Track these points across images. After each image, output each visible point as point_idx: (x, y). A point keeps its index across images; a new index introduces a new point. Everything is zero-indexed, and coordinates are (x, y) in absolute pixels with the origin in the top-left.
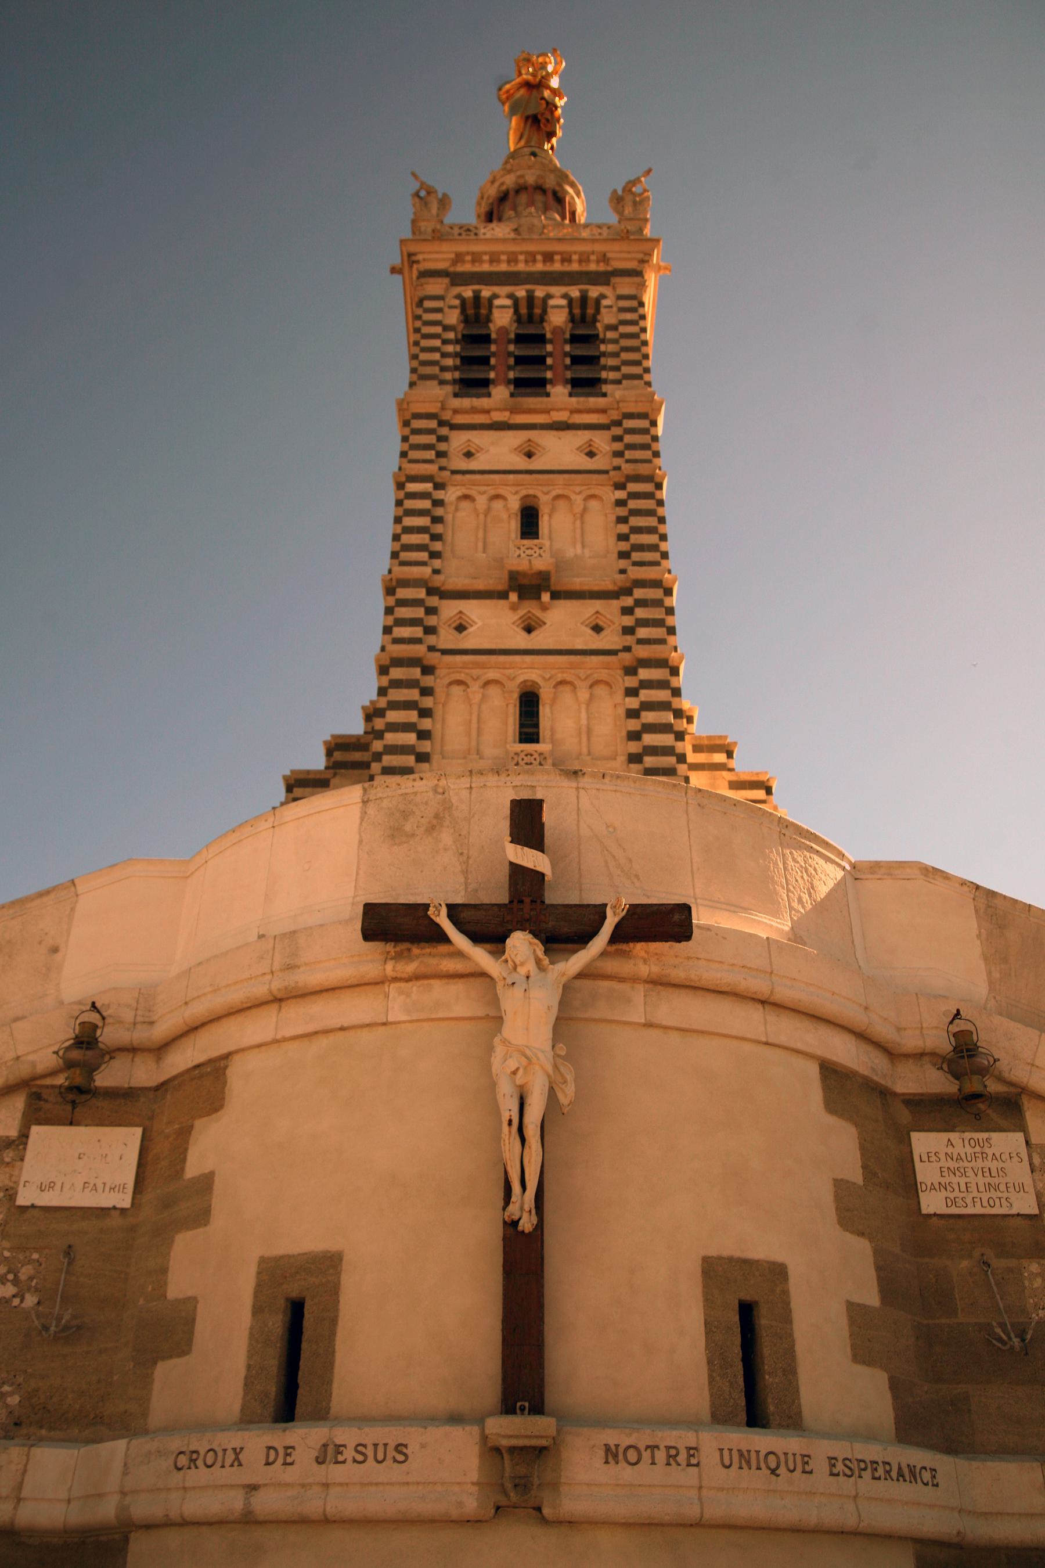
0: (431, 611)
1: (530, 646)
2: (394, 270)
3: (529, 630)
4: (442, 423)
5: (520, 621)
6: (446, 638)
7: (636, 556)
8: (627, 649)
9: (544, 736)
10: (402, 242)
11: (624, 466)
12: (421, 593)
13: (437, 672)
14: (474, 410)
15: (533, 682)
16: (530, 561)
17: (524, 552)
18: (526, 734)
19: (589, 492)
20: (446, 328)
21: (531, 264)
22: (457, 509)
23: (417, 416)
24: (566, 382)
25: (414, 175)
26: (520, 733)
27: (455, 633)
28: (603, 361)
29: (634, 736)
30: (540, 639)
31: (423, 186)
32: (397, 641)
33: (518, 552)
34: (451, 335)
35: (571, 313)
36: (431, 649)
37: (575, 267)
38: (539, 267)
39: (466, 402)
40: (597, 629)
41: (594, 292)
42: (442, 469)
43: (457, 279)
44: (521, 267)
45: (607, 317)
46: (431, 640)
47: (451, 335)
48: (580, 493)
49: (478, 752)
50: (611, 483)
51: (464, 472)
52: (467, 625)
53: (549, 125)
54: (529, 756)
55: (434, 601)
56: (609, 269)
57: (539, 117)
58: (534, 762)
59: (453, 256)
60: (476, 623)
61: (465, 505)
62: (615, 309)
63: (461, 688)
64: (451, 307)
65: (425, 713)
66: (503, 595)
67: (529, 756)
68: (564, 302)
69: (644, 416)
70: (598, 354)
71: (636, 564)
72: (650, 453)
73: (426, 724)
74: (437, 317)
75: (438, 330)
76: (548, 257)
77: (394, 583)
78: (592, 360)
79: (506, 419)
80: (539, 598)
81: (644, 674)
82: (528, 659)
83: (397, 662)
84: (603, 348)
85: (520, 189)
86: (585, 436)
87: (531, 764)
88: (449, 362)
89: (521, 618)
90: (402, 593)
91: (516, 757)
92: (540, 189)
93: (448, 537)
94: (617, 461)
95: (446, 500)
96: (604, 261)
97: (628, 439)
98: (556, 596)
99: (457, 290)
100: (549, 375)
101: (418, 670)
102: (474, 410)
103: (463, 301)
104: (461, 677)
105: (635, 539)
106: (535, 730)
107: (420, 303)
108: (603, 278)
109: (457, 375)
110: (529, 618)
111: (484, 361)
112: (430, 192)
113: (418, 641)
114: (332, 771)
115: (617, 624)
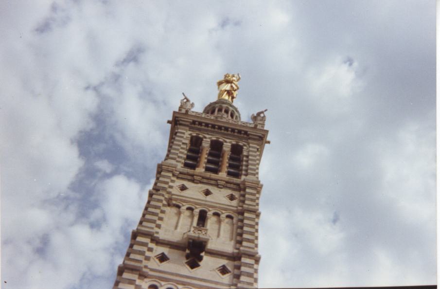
0: (150, 250)
2: (169, 122)
10: (174, 112)
14: (188, 174)
20: (183, 143)
25: (183, 94)
28: (241, 168)
31: (186, 98)
36: (146, 267)
43: (191, 129)
47: (184, 146)
55: (151, 245)
59: (191, 121)
69: (255, 188)
78: (238, 167)
90: (139, 239)
99: (190, 132)
103: (192, 137)
107: (176, 133)
112: (188, 101)
115: (232, 272)
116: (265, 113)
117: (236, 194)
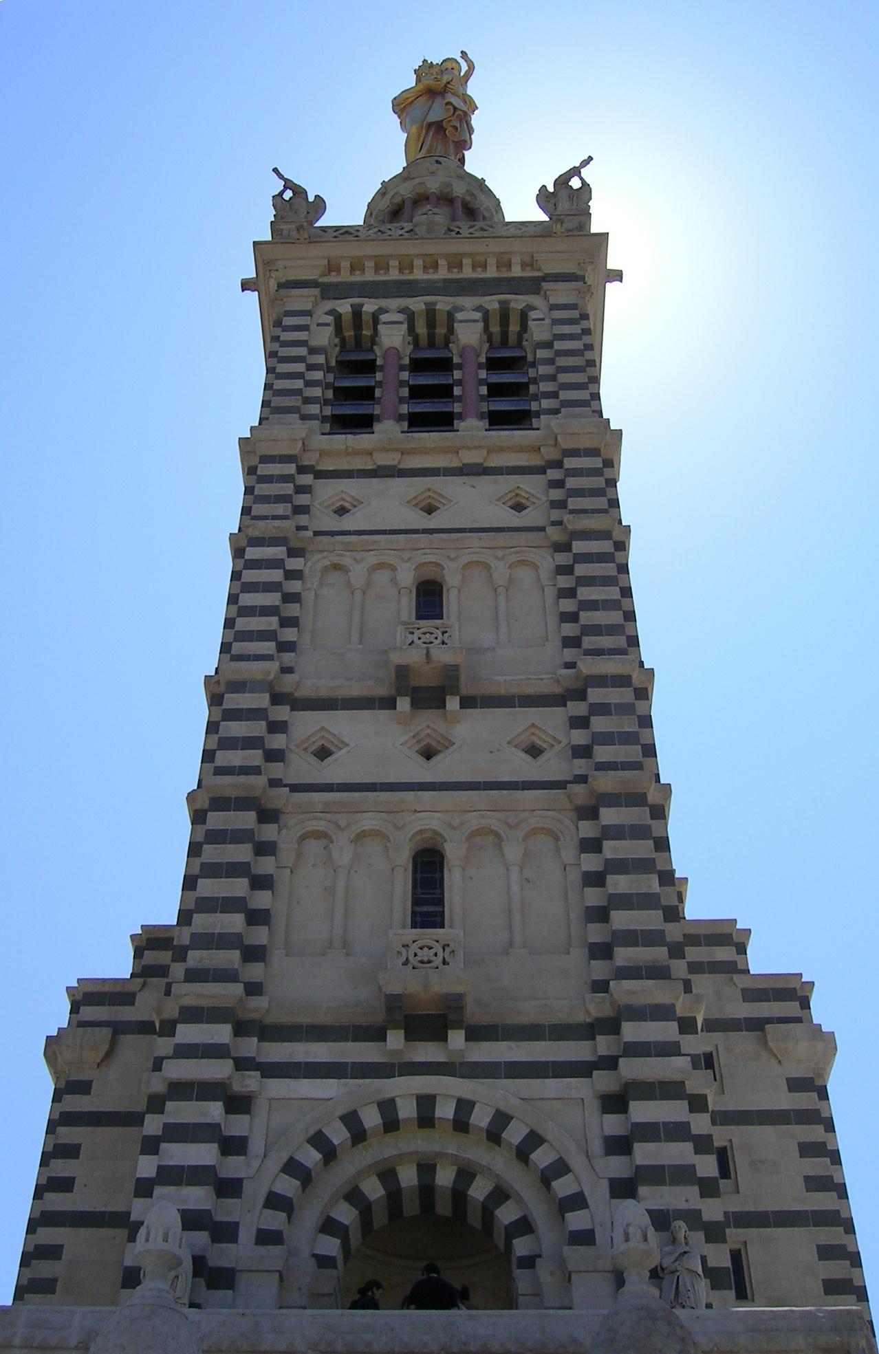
0: (277, 727)
1: (427, 778)
2: (246, 285)
3: (428, 754)
4: (302, 470)
5: (415, 741)
6: (301, 768)
7: (588, 642)
8: (582, 779)
9: (451, 917)
11: (566, 518)
12: (261, 700)
13: (283, 819)
15: (436, 833)
16: (428, 648)
17: (419, 638)
18: (423, 914)
19: (515, 558)
20: (313, 351)
21: (431, 271)
22: (321, 585)
23: (266, 459)
24: (481, 416)
25: (275, 170)
26: (414, 914)
27: (314, 760)
28: (532, 389)
29: (600, 915)
30: (442, 769)
31: (288, 184)
32: (221, 771)
33: (410, 638)
34: (320, 359)
35: (486, 328)
36: (274, 783)
37: (491, 272)
38: (443, 273)
39: (342, 441)
40: (534, 751)
41: (518, 302)
42: (299, 528)
43: (330, 291)
44: (418, 274)
45: (538, 331)
46: (276, 770)
47: (320, 359)
48: (503, 557)
49: (345, 943)
50: (550, 545)
51: (332, 534)
52: (333, 748)
53: (457, 134)
54: (425, 949)
55: (282, 713)
56: (537, 274)
57: (444, 124)
58: (433, 958)
59: (326, 262)
60: (348, 745)
61: (335, 578)
62: (547, 321)
63: (323, 842)
64: (319, 325)
65: (261, 883)
66: (388, 703)
67: (426, 949)
68: (478, 315)
70: (525, 380)
71: (588, 652)
72: (604, 500)
73: (262, 899)
74: (302, 335)
75: (302, 351)
76: (455, 263)
77: (222, 688)
79: (396, 462)
80: (442, 705)
81: (609, 816)
82: (427, 795)
83: (220, 803)
84: (532, 373)
85: (421, 199)
86: (514, 480)
87: (429, 962)
88: (317, 392)
89: (414, 737)
91: (404, 951)
92: (446, 199)
93: (306, 621)
94: (556, 515)
95: (307, 571)
96: (532, 265)
97: (572, 483)
98: (468, 702)
99: (329, 305)
100: (457, 408)
101: (252, 815)
102: (348, 452)
104: (321, 826)
105: (586, 617)
106: (438, 909)
108: (533, 285)
109: (328, 411)
110: (428, 735)
111: (367, 394)
112: (299, 192)
113: (256, 771)
114: (141, 980)
116: (584, 172)
117: (532, 485)
